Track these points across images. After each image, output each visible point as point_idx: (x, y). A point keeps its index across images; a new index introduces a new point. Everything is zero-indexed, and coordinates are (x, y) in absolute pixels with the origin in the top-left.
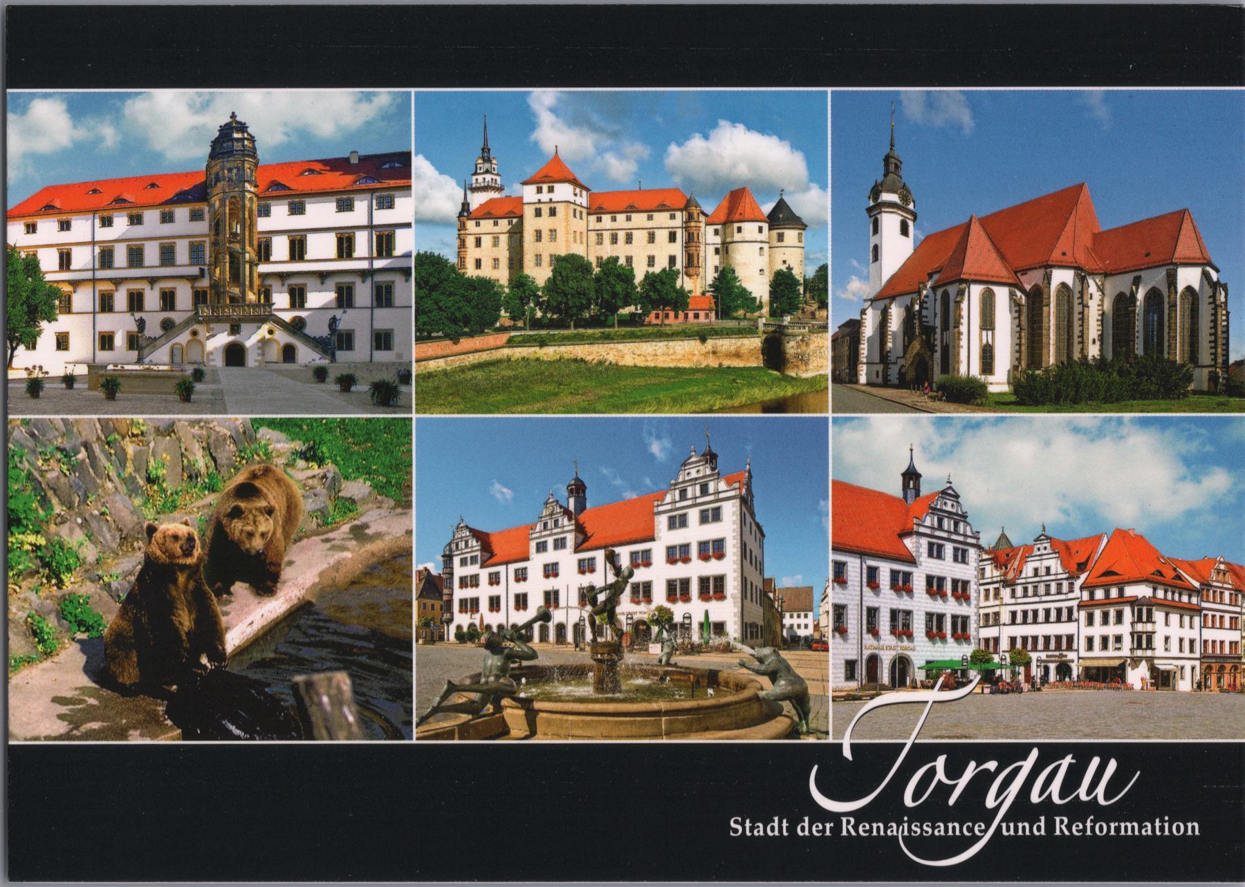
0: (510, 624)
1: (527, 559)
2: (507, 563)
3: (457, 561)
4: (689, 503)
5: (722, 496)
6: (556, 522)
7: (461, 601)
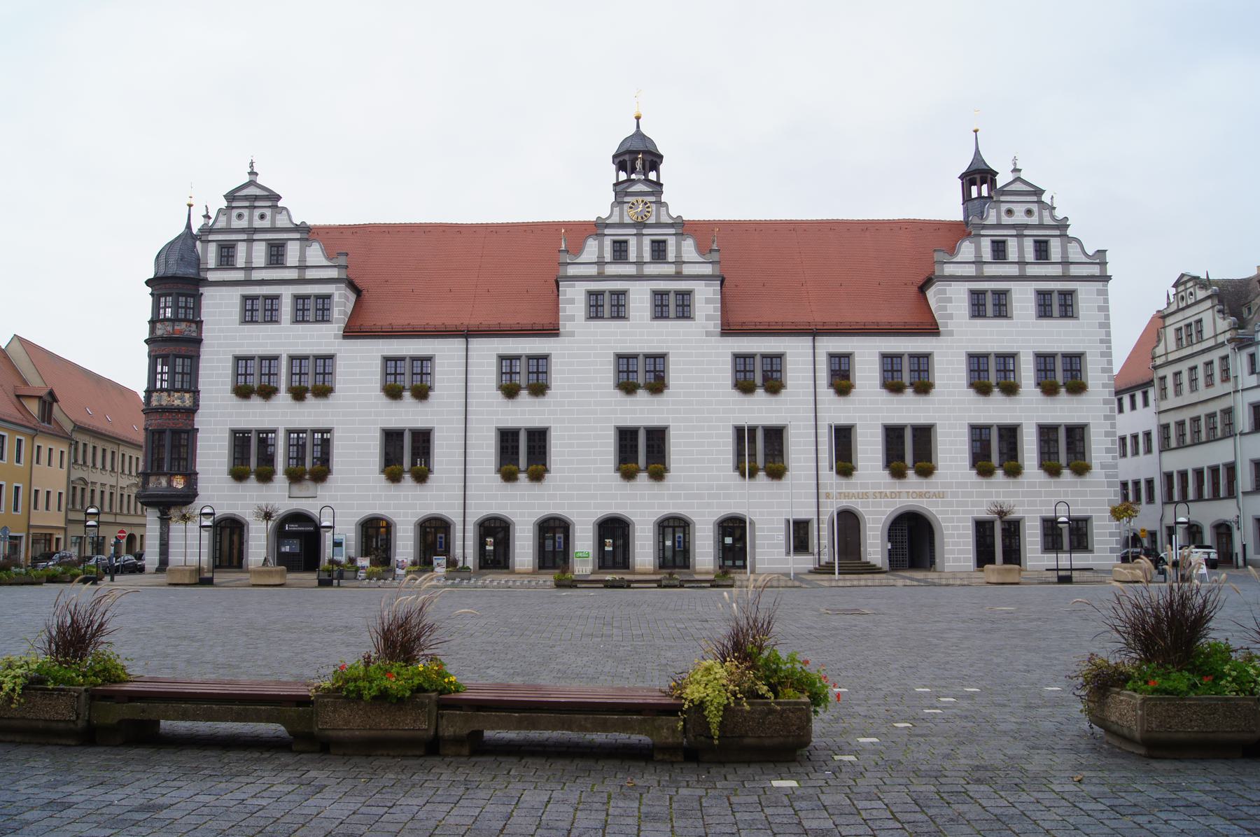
0: (478, 512)
1: (552, 331)
2: (467, 334)
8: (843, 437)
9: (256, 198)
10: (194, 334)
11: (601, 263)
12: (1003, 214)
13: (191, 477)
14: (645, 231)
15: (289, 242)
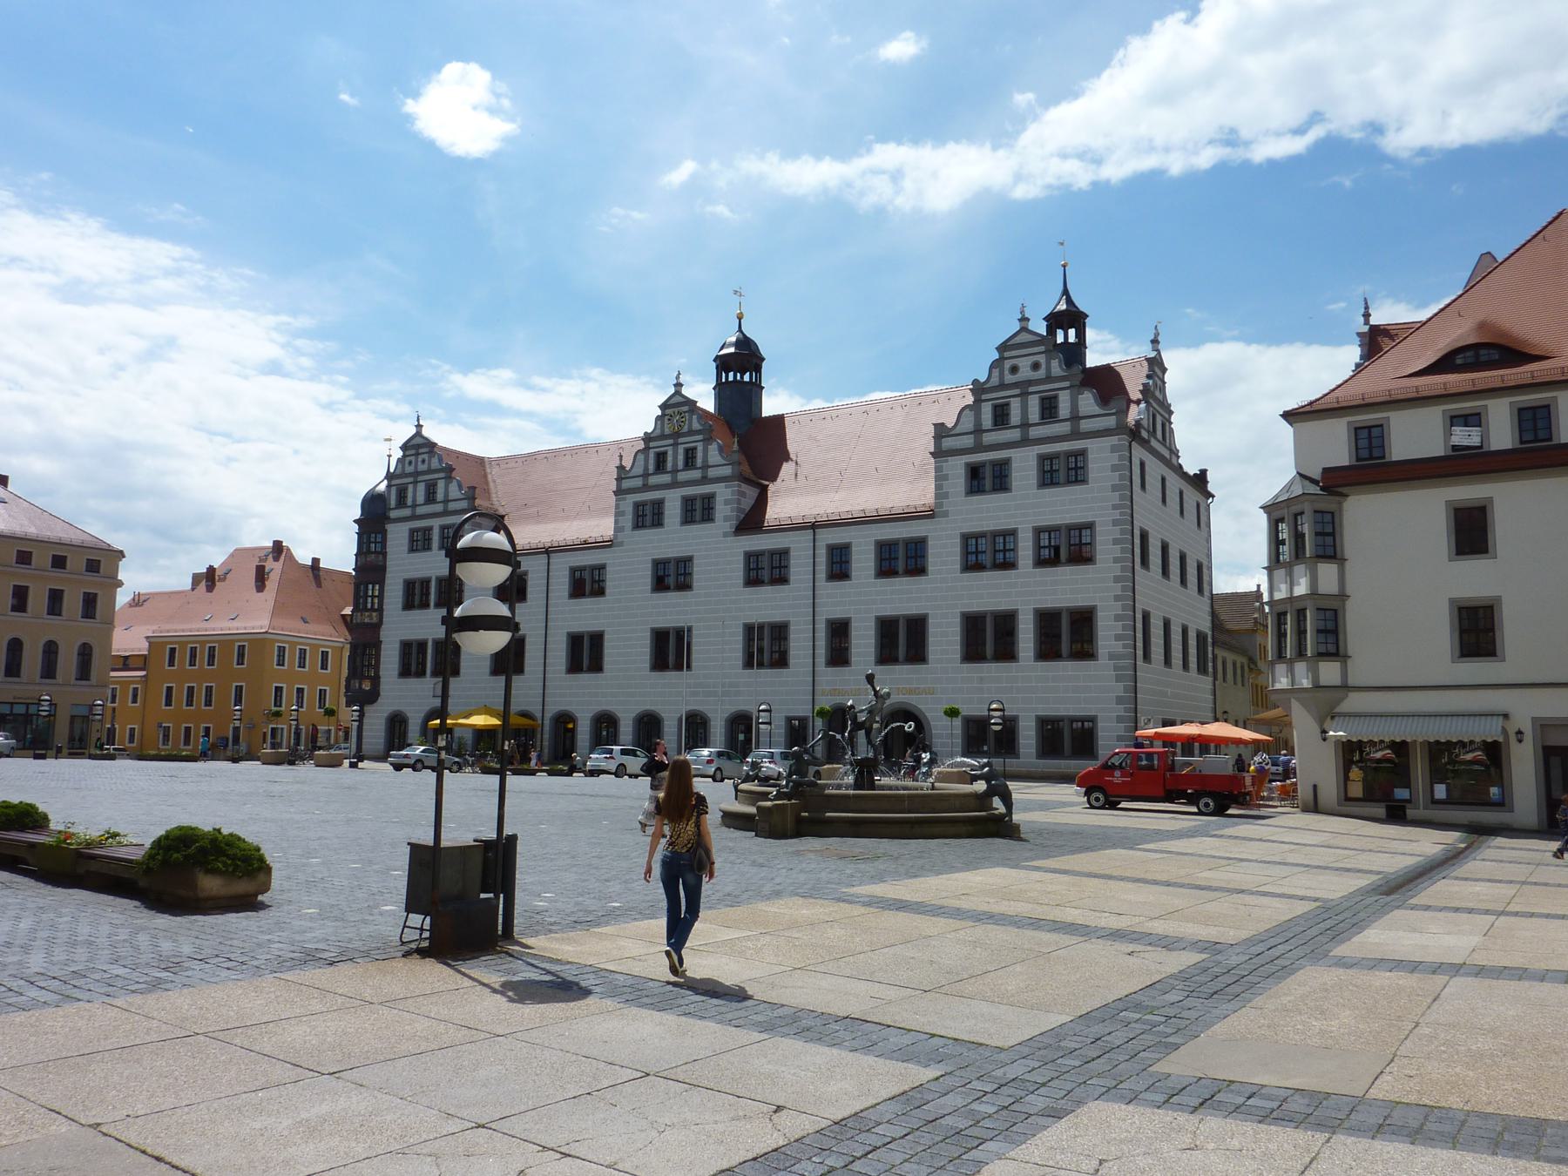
0: (552, 710)
3: (397, 535)
4: (1014, 435)
5: (1085, 425)
6: (690, 455)
7: (406, 647)
8: (839, 631)
9: (419, 446)
10: (381, 564)
11: (646, 475)
12: (1006, 372)
13: (376, 681)
14: (681, 440)
15: (439, 481)
